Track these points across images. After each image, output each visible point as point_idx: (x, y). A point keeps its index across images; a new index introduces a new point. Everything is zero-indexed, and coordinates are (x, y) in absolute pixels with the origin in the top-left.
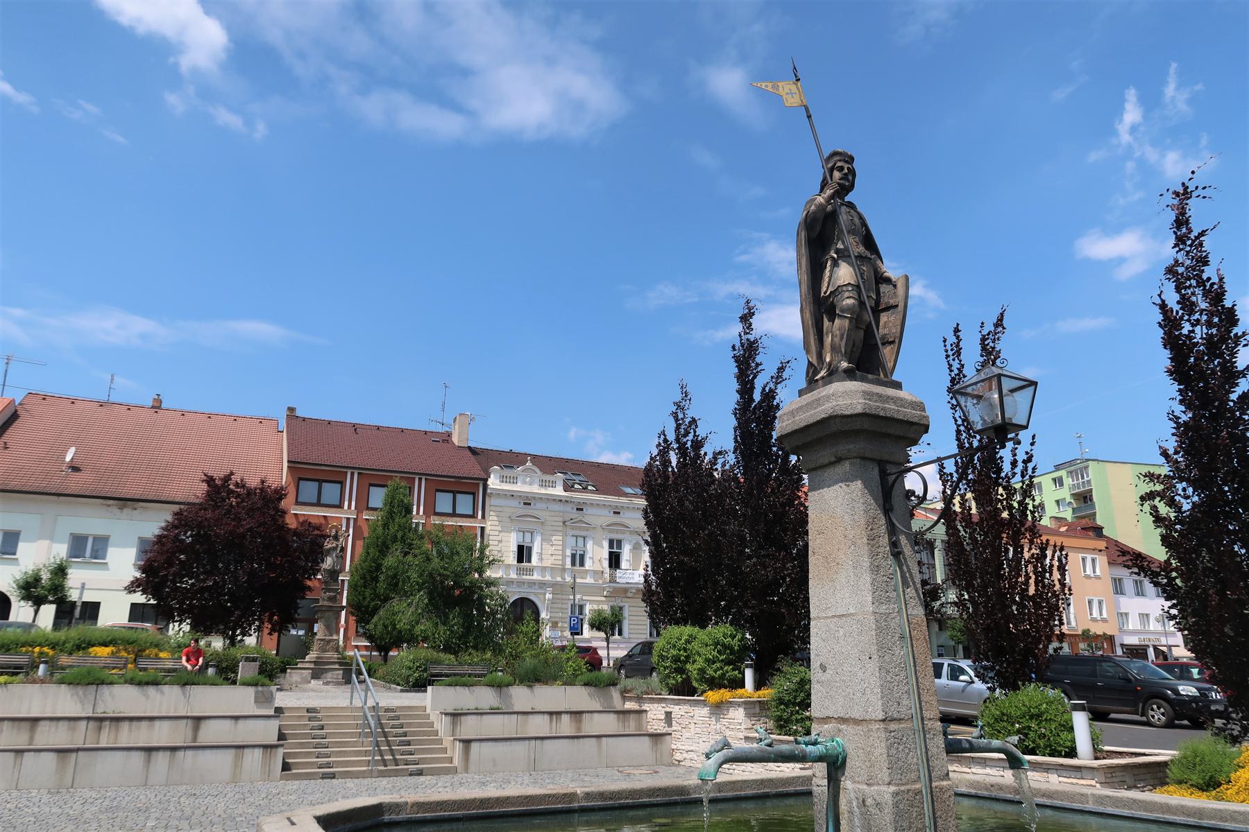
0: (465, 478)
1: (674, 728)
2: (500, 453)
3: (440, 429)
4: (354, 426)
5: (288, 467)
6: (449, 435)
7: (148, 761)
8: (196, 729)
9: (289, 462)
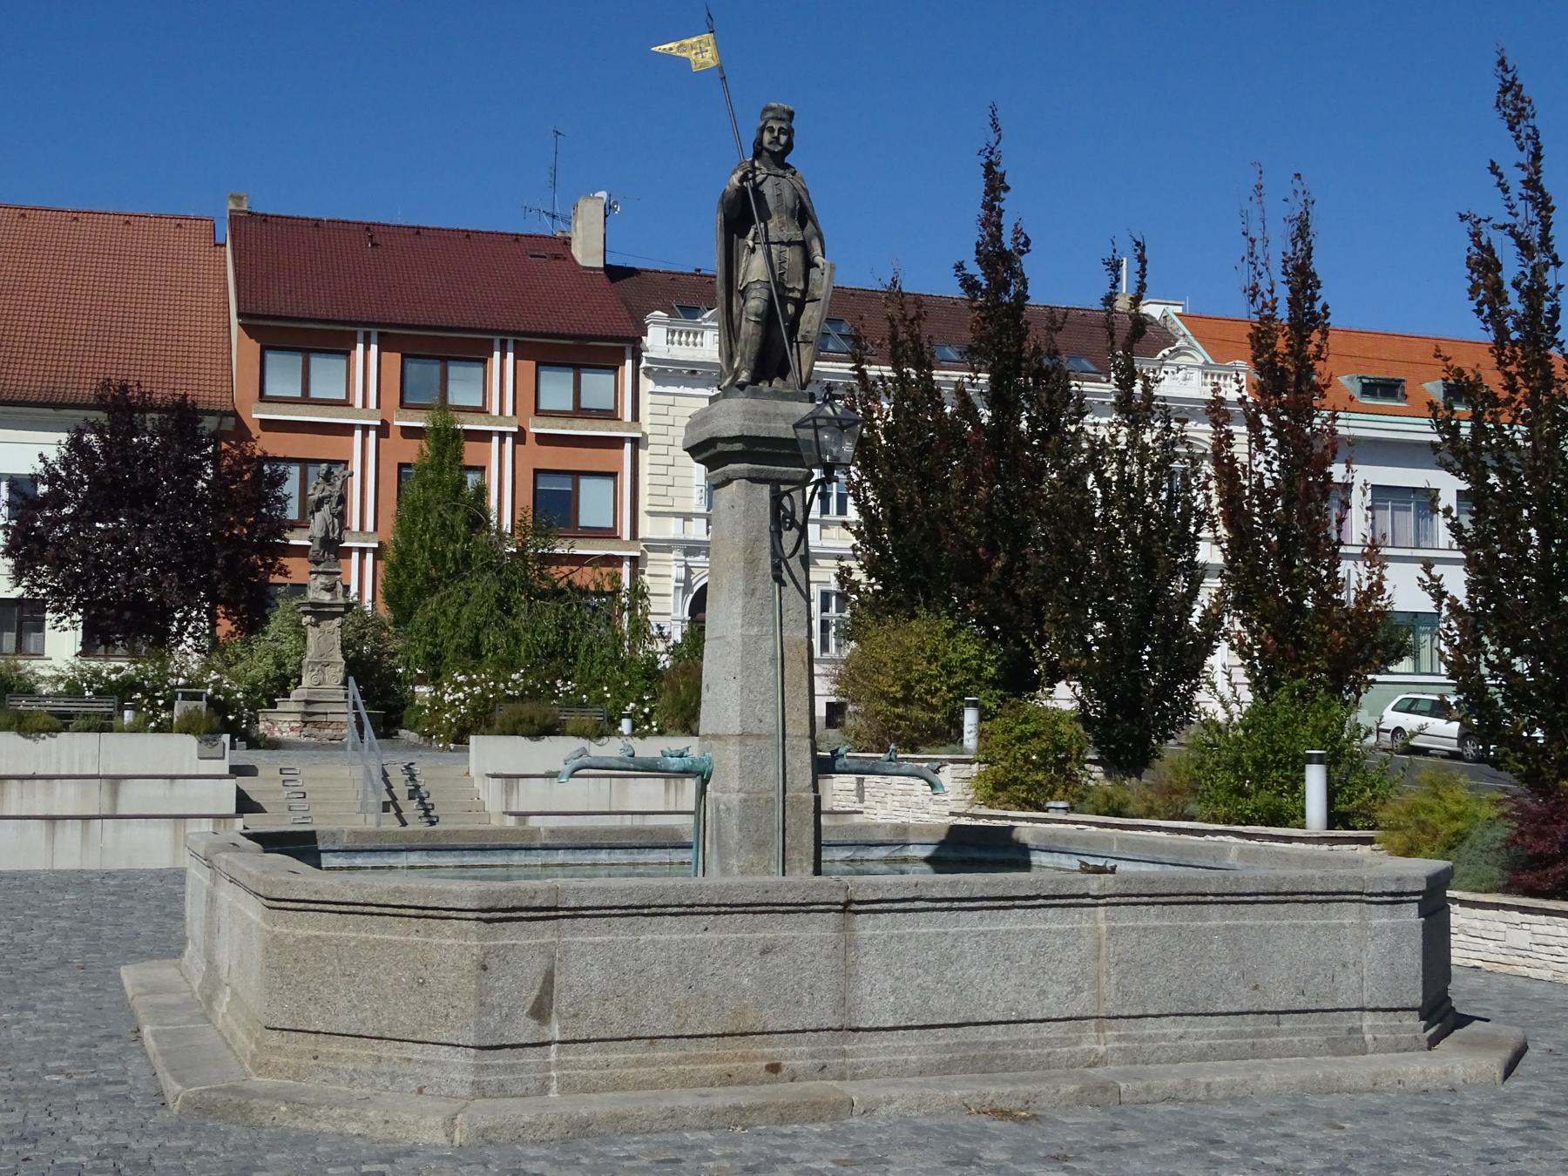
0: (595, 338)
1: (866, 803)
2: (674, 276)
3: (544, 227)
4: (368, 229)
5: (240, 324)
6: (567, 242)
7: (51, 836)
8: (115, 794)
9: (239, 315)
